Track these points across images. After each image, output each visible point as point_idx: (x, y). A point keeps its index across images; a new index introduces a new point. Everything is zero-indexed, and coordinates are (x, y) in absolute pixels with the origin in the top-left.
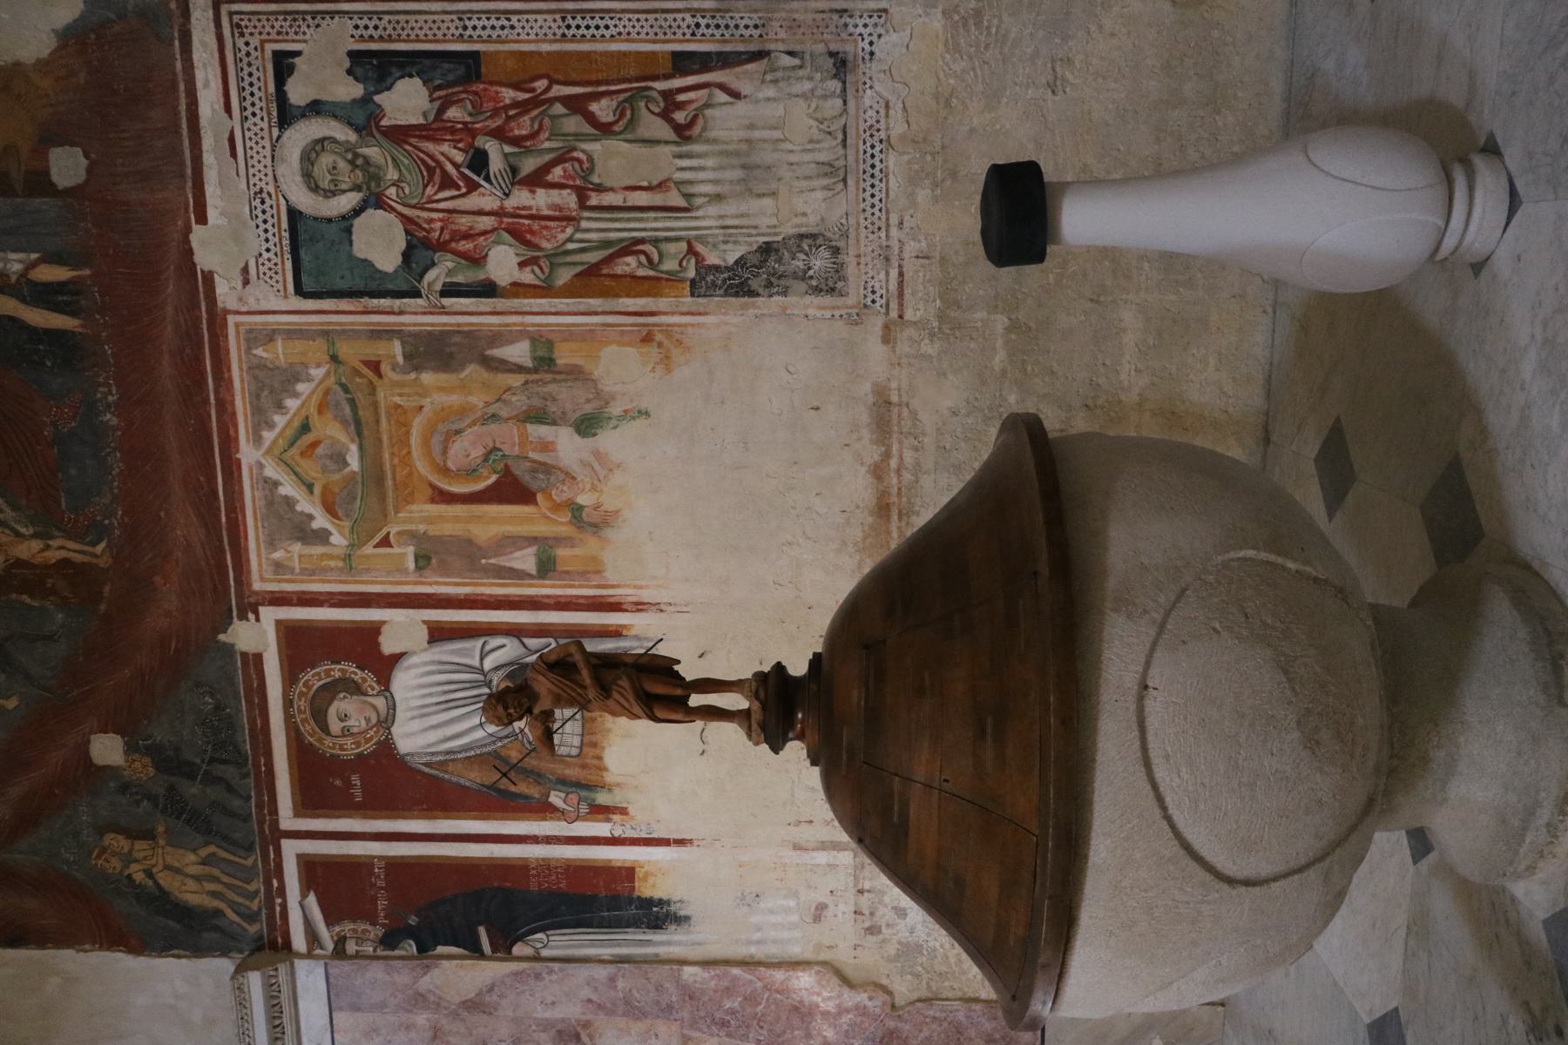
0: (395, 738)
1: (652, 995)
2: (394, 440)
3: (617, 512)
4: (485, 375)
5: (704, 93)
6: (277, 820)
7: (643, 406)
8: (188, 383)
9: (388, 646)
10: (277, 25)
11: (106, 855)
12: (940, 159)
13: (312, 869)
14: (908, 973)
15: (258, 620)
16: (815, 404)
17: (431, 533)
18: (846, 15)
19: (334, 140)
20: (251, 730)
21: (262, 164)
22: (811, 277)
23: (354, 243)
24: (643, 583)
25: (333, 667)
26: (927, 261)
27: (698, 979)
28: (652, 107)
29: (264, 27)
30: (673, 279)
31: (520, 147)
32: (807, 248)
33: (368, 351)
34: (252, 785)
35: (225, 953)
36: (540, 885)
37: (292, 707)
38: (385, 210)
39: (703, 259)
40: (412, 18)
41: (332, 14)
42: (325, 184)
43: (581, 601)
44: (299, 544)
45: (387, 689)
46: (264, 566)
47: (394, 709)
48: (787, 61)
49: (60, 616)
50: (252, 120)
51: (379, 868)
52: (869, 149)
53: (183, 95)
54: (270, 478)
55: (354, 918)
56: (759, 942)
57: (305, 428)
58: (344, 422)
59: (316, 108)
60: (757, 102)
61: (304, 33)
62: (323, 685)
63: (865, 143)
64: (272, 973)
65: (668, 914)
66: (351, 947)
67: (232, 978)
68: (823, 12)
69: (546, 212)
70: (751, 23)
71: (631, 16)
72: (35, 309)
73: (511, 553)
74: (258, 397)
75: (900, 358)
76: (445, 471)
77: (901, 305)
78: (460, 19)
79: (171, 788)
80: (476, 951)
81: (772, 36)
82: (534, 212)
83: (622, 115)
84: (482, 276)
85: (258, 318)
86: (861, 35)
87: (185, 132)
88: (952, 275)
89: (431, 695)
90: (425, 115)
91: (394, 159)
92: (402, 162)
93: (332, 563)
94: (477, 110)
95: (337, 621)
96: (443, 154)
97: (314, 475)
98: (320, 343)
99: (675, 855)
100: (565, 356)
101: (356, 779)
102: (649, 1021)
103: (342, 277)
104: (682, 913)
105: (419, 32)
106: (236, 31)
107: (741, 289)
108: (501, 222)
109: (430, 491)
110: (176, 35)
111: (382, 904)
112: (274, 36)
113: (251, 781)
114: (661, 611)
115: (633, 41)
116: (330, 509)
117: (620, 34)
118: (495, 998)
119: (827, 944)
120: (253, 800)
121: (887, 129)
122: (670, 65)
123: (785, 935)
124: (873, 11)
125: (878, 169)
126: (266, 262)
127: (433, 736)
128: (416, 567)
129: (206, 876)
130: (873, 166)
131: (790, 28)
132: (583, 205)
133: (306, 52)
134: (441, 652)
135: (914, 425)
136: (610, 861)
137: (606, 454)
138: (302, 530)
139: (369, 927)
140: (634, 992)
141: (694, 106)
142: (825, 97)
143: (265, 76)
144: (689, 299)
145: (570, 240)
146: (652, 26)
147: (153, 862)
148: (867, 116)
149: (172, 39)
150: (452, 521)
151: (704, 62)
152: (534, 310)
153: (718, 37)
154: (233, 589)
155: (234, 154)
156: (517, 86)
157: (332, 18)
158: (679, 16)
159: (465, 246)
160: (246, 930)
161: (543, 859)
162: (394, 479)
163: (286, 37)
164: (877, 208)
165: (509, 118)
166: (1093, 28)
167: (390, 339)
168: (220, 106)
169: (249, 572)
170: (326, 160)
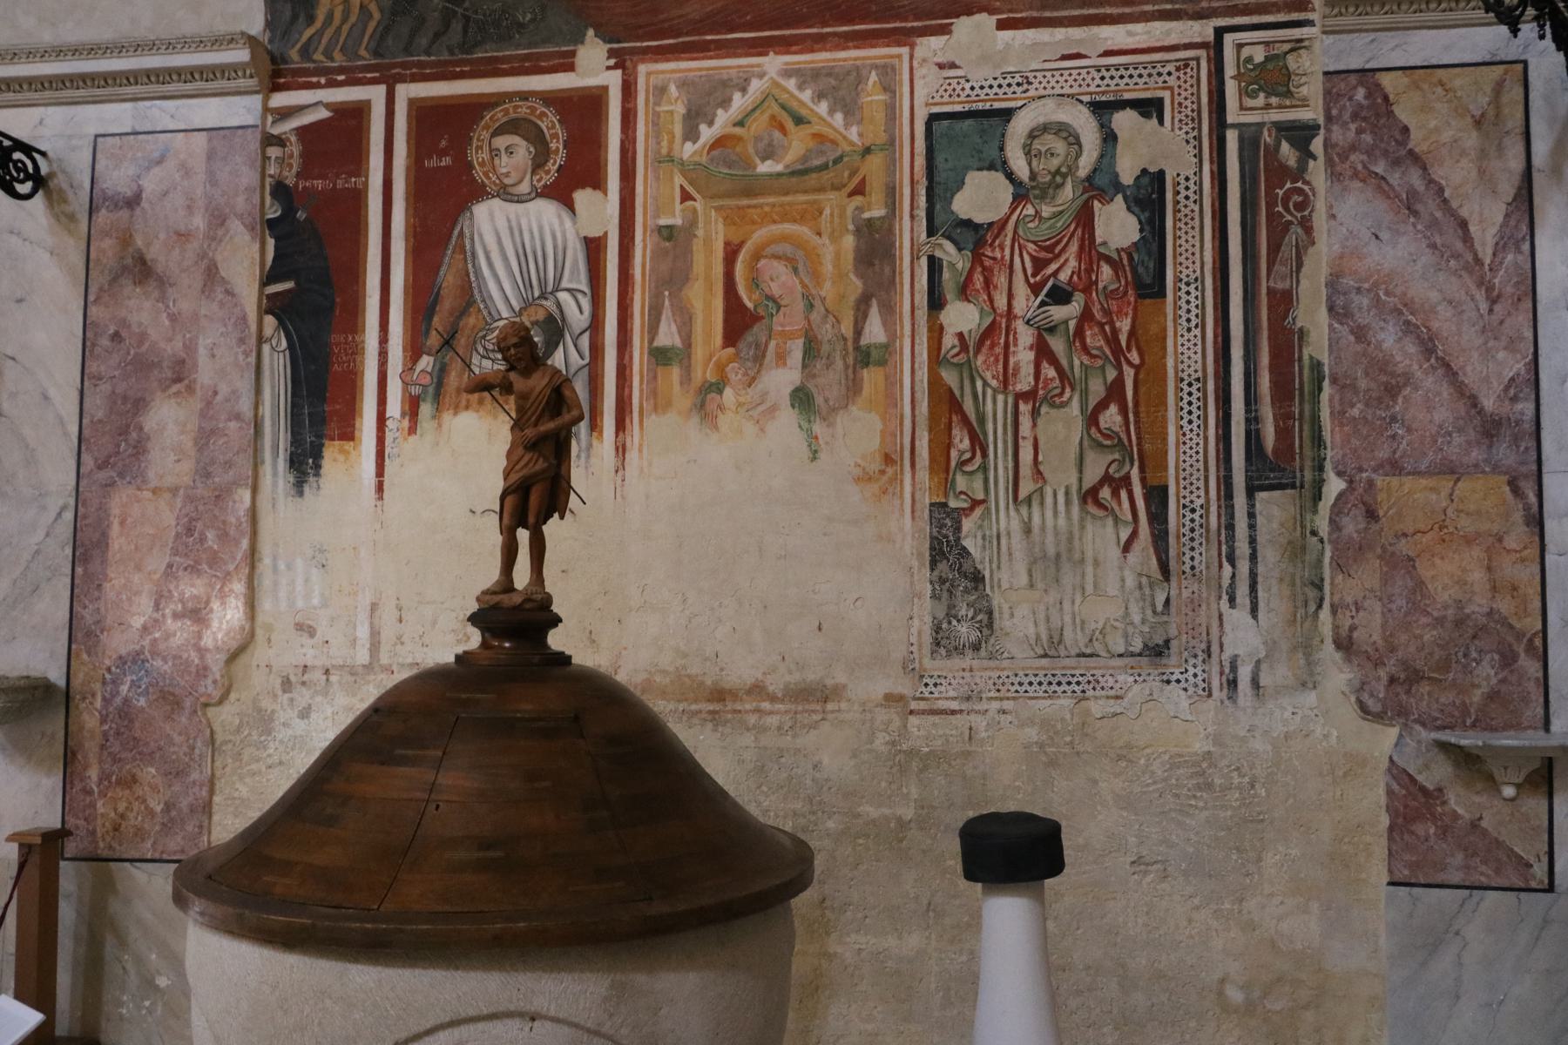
2: (787, 208)
3: (716, 428)
4: (852, 299)
5: (1129, 517)
6: (404, 81)
7: (822, 455)
8: (843, 7)
9: (582, 197)
12: (1067, 750)
13: (355, 115)
14: (241, 721)
15: (609, 68)
16: (824, 627)
17: (695, 240)
18: (1205, 656)
19: (1079, 154)
22: (950, 623)
24: (645, 451)
26: (967, 738)
28: (1114, 466)
30: (947, 485)
31: (1075, 336)
32: (979, 618)
35: (269, 24)
36: (337, 344)
39: (967, 516)
40: (1197, 233)
41: (1199, 156)
42: (1037, 145)
43: (627, 390)
46: (661, 76)
47: (518, 202)
48: (1160, 599)
50: (1097, 76)
52: (1075, 679)
55: (306, 156)
56: (275, 569)
57: (799, 121)
58: (805, 158)
59: (1109, 138)
60: (1121, 569)
61: (1180, 129)
62: (542, 131)
63: (1082, 675)
64: (248, 72)
65: (305, 474)
66: (273, 152)
67: (243, 33)
68: (1208, 634)
69: (1012, 360)
70: (1196, 563)
71: (1201, 445)
74: (829, 75)
75: (870, 711)
76: (757, 256)
77: (923, 712)
78: (1196, 280)
80: (269, 278)
81: (1184, 583)
82: (1012, 349)
84: (948, 297)
85: (906, 76)
86: (1186, 671)
87: (1085, 12)
88: (953, 763)
89: (532, 238)
90: (1104, 244)
91: (1061, 212)
93: (665, 143)
94: (1109, 295)
95: (607, 147)
96: (1067, 260)
97: (753, 128)
98: (882, 138)
99: (366, 482)
100: (871, 378)
101: (446, 161)
102: (193, 453)
103: (946, 160)
104: (306, 488)
105: (1183, 239)
106: (1182, 63)
108: (1001, 316)
110: (1177, 6)
113: (446, 57)
116: (719, 143)
117: (1184, 435)
118: (220, 296)
119: (272, 638)
121: (1096, 698)
122: (1155, 484)
123: (282, 594)
124: (1209, 683)
125: (1057, 688)
127: (490, 240)
130: (1059, 684)
131: (1192, 601)
132: (1020, 396)
133: (1163, 130)
135: (804, 726)
136: (361, 417)
137: (773, 418)
138: (698, 114)
139: (294, 170)
140: (225, 439)
142: (1126, 636)
144: (927, 501)
145: (985, 384)
146: (1191, 466)
148: (1107, 677)
150: (707, 261)
151: (1158, 517)
152: (916, 347)
153: (1183, 530)
154: (638, 44)
155: (1064, 58)
156: (1132, 333)
158: (1202, 493)
159: (978, 280)
160: (293, 46)
161: (363, 348)
162: (749, 207)
164: (1019, 688)
165: (1101, 325)
166: (1196, 901)
168: (1110, 45)
169: (656, 61)
170: (1060, 147)
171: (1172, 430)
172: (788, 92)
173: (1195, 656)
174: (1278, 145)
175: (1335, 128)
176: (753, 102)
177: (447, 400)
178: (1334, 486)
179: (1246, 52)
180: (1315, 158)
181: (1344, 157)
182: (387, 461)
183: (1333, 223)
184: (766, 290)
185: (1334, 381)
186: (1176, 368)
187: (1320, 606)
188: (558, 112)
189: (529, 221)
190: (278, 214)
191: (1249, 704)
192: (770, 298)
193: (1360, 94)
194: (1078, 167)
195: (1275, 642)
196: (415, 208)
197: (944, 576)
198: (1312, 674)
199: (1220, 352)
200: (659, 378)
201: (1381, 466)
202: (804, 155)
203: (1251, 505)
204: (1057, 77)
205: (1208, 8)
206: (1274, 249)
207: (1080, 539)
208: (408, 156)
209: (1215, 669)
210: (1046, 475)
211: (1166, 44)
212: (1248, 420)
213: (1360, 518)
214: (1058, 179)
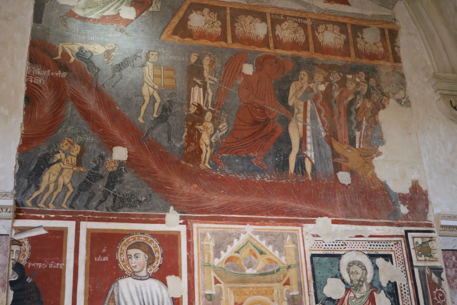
0: (126, 279)
6: (86, 221)
8: (274, 209)
9: (170, 279)
10: (400, 257)
11: (70, 144)
15: (180, 224)
17: (222, 301)
20: (129, 214)
21: (355, 246)
23: (332, 279)
25: (160, 254)
29: (399, 252)
34: (103, 212)
35: (16, 188)
37: (141, 234)
38: (346, 292)
42: (351, 269)
44: (214, 245)
45: (150, 277)
46: (203, 229)
47: (140, 280)
49: (179, 146)
50: (369, 244)
51: (59, 266)
54: (240, 236)
55: (32, 251)
57: (261, 253)
58: (265, 269)
59: (376, 268)
61: (399, 266)
62: (151, 248)
64: (9, 210)
66: (15, 248)
72: (295, 158)
74: (272, 235)
79: (102, 177)
85: (301, 239)
89: (148, 297)
91: (363, 296)
92: (363, 299)
93: (206, 258)
97: (243, 254)
98: (294, 262)
101: (106, 259)
103: (319, 273)
110: (391, 221)
111: (40, 265)
112: (397, 255)
113: (105, 211)
116: (229, 259)
120: (96, 211)
126: (321, 244)
127: (127, 296)
128: (206, 294)
129: (57, 186)
138: (220, 246)
139: (26, 258)
143: (383, 251)
149: (389, 220)
154: (193, 215)
155: (357, 236)
157: (405, 277)
160: (28, 199)
162: (244, 288)
163: (397, 260)
167: (299, 291)
169: (201, 223)
170: (360, 270)
172: (256, 241)
174: (432, 274)
175: (448, 270)
176: (242, 244)
179: (416, 240)
180: (444, 281)
188: (158, 240)
189: (146, 289)
194: (367, 279)
196: (90, 280)
202: (265, 267)
204: (355, 244)
205: (402, 223)
208: (87, 254)
211: (390, 234)
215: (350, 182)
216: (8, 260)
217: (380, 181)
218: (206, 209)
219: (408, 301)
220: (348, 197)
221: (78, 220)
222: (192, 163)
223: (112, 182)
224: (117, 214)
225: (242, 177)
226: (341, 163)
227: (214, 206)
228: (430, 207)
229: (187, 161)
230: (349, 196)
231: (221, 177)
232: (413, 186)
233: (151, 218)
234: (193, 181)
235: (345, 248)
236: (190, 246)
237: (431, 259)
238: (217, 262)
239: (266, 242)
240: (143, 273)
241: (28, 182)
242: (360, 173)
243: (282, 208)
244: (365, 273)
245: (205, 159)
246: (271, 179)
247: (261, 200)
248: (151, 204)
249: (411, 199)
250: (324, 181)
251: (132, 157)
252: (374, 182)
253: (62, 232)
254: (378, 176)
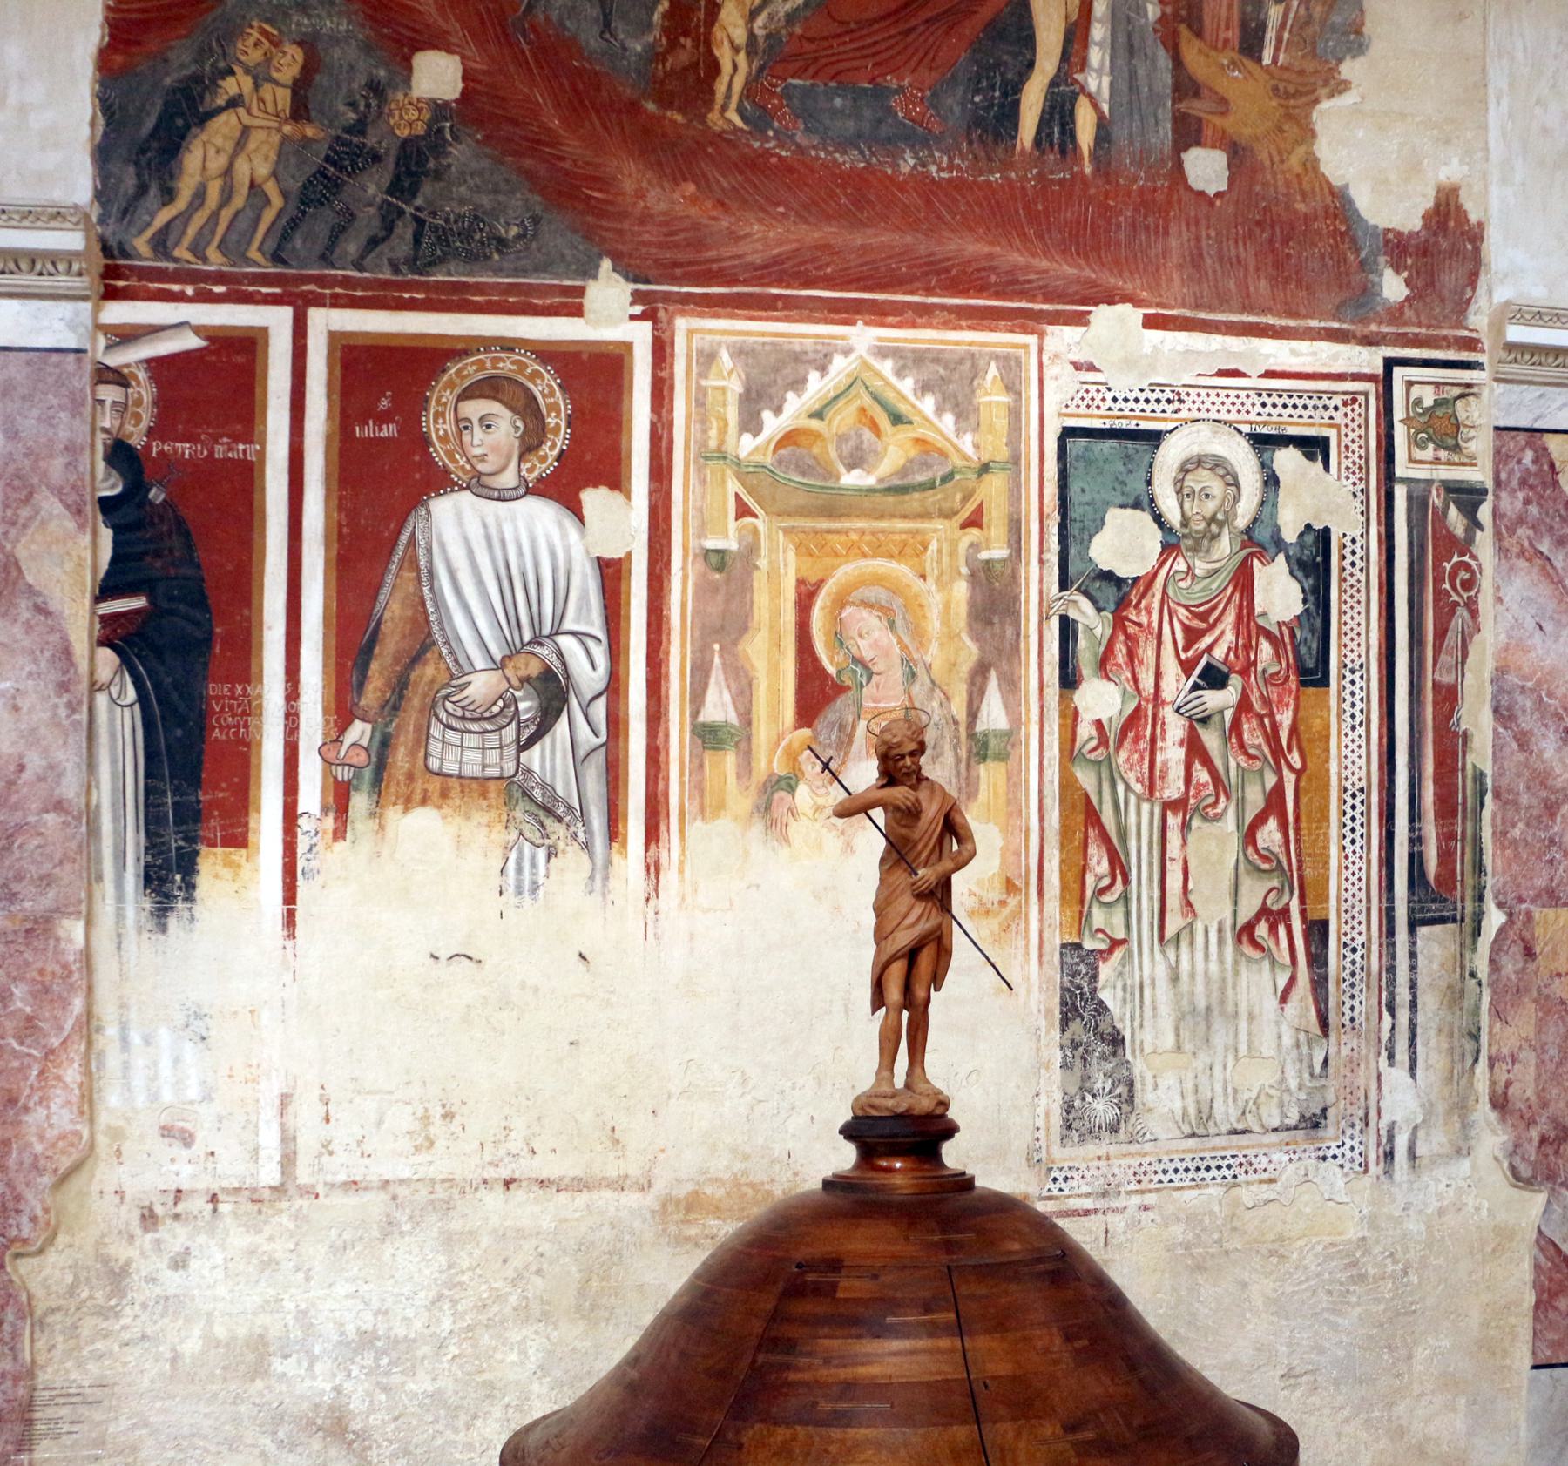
0: (455, 495)
1: (33, 868)
3: (787, 841)
4: (966, 667)
6: (324, 305)
8: (954, 272)
9: (594, 499)
10: (1354, 447)
11: (267, 44)
15: (633, 318)
17: (756, 574)
19: (1237, 499)
23: (1122, 511)
27: (63, 944)
30: (1082, 921)
32: (1118, 1091)
33: (994, 514)
34: (381, 276)
35: (100, 195)
36: (218, 699)
37: (503, 349)
39: (1105, 960)
40: (1362, 608)
42: (1190, 482)
43: (661, 786)
45: (529, 492)
46: (708, 337)
47: (498, 499)
50: (1258, 401)
51: (245, 451)
53: (1284, 322)
57: (897, 419)
58: (904, 471)
59: (1271, 481)
60: (1277, 1023)
62: (535, 399)
66: (109, 393)
69: (1159, 759)
73: (728, 687)
74: (936, 360)
76: (840, 602)
79: (376, 158)
80: (106, 591)
81: (1344, 1038)
82: (1159, 744)
83: (1265, 858)
89: (521, 554)
90: (1264, 614)
91: (1217, 571)
93: (713, 433)
94: (1270, 679)
95: (630, 430)
96: (1222, 633)
97: (835, 423)
98: (1004, 453)
101: (389, 431)
103: (1083, 491)
107: (1070, 1010)
109: (813, 579)
110: (1345, 326)
111: (186, 449)
112: (1345, 441)
113: (386, 275)
114: (648, 900)
115: (1339, 874)
116: (789, 438)
117: (1347, 857)
118: (26, 615)
128: (708, 551)
129: (231, 188)
132: (1168, 806)
134: (584, 576)
136: (258, 811)
138: (760, 395)
141: (1273, 947)
142: (1281, 1105)
144: (1058, 942)
145: (1128, 788)
147: (255, 111)
149: (1339, 320)
151: (1318, 959)
152: (1046, 737)
154: (676, 289)
155: (1222, 373)
156: (1294, 730)
158: (1363, 928)
160: (140, 233)
161: (260, 706)
162: (829, 532)
165: (1261, 718)
167: (1010, 546)
169: (701, 315)
170: (1216, 487)
171: (1334, 851)
172: (883, 378)
173: (1353, 1126)
174: (1447, 507)
175: (1503, 494)
176: (835, 387)
177: (392, 789)
178: (1494, 919)
179: (1416, 391)
180: (1482, 529)
181: (1512, 531)
182: (300, 882)
183: (1499, 607)
184: (854, 650)
185: (1497, 795)
186: (1339, 774)
187: (1476, 1060)
189: (516, 529)
190: (118, 490)
191: (1405, 1178)
192: (858, 661)
193: (1528, 456)
195: (1432, 1105)
196: (340, 498)
197: (1077, 1039)
198: (1466, 1138)
199: (1385, 758)
200: (707, 764)
201: (1538, 896)
202: (904, 467)
203: (1413, 943)
204: (1213, 398)
205: (1377, 333)
206: (1440, 634)
207: (1234, 988)
209: (1373, 1140)
210: (1197, 906)
211: (1333, 370)
212: (1411, 841)
213: (1518, 957)
214: (1214, 528)
215: (1223, 187)
216: (87, 429)
217: (1329, 183)
218: (720, 269)
219: (1359, 591)
220: (1208, 237)
221: (300, 302)
222: (680, 110)
223: (410, 174)
224: (427, 283)
225: (849, 160)
226: (1202, 115)
227: (749, 259)
228: (1483, 280)
229: (665, 101)
230: (1213, 234)
231: (780, 157)
232: (1437, 205)
233: (539, 298)
234: (680, 170)
235: (1177, 411)
236: (661, 392)
237: (1456, 459)
238: (747, 445)
239: (916, 382)
240: (508, 479)
241: (138, 175)
242: (1263, 156)
243: (979, 270)
244: (1231, 498)
245: (728, 96)
246: (950, 168)
247: (909, 239)
248: (539, 250)
249: (1424, 251)
250: (1135, 179)
251: (478, 87)
252: (1307, 187)
253: (249, 345)
254: (1326, 169)
